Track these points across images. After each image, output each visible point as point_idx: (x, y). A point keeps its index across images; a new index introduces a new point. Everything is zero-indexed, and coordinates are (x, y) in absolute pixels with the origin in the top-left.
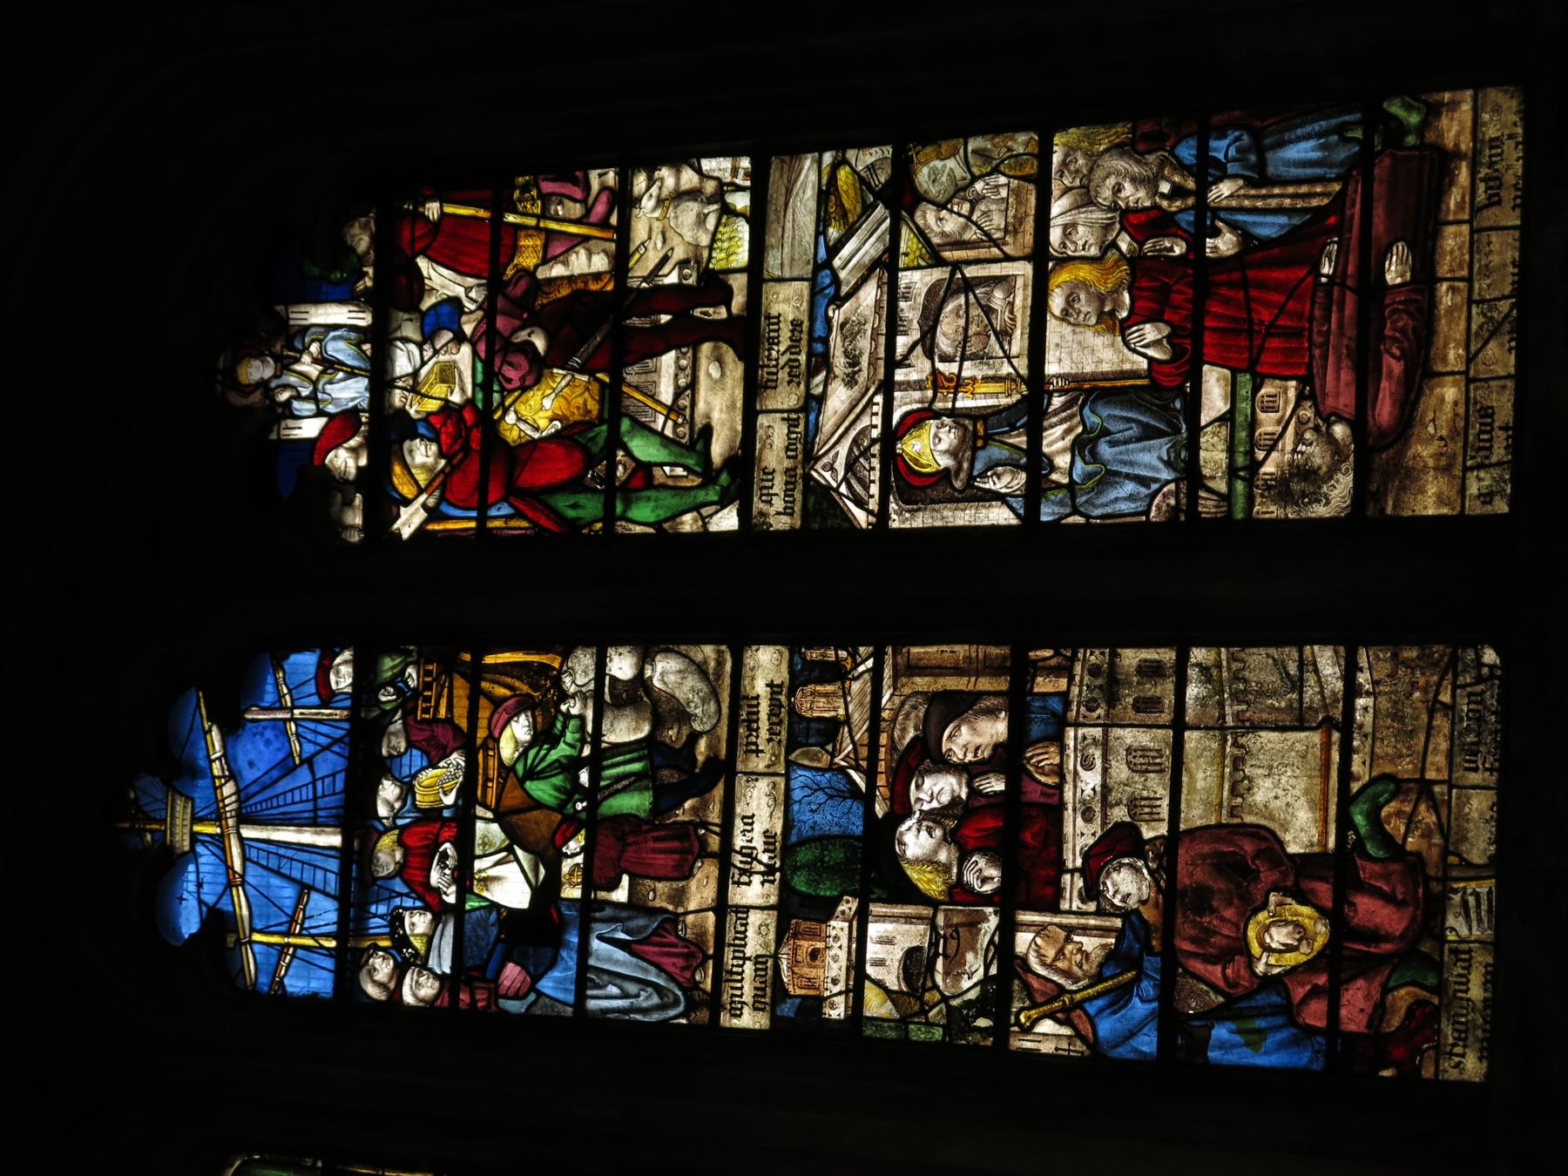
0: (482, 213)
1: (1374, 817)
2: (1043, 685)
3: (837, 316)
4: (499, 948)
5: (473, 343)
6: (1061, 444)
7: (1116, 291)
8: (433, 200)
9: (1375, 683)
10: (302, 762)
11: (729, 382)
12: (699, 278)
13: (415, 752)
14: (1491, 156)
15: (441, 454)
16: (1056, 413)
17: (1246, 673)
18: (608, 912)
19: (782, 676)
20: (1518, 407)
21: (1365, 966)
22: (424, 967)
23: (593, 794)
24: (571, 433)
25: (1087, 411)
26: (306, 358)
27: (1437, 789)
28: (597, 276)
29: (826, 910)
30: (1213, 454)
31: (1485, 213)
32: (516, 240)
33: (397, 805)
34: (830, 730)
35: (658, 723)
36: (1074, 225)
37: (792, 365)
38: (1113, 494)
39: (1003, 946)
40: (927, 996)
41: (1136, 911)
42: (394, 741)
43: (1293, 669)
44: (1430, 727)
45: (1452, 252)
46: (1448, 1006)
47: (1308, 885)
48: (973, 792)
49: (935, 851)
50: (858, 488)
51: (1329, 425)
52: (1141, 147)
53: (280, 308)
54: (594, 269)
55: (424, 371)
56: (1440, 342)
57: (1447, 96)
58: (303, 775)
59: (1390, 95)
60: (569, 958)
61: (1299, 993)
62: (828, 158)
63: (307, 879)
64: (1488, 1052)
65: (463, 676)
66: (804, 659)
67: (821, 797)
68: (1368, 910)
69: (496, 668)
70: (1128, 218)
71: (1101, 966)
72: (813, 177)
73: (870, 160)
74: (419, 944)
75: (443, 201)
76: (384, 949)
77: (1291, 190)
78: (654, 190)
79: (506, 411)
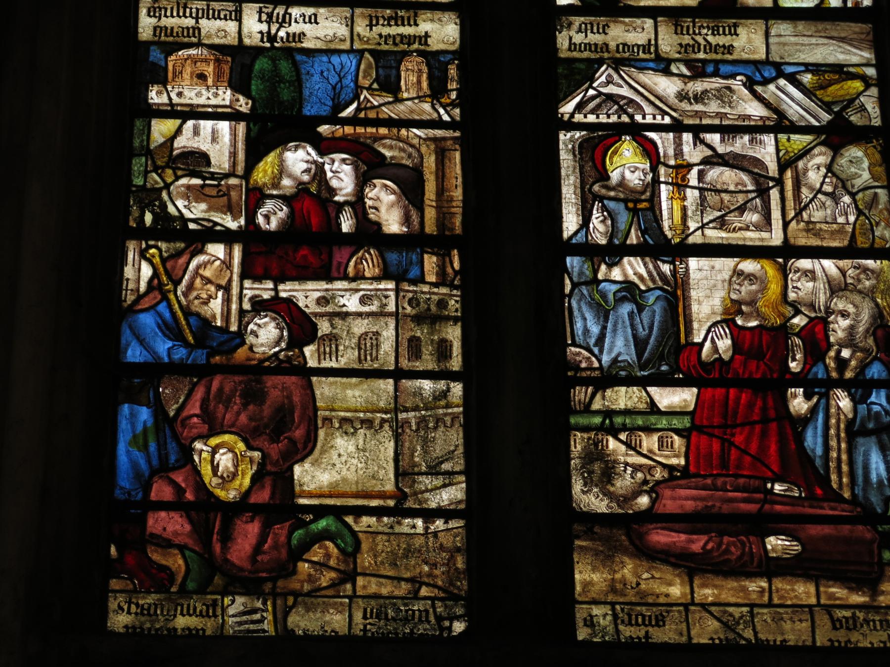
2: (430, 262)
3: (737, 84)
6: (630, 272)
7: (759, 315)
9: (435, 534)
14: (874, 621)
16: (657, 268)
17: (442, 429)
19: (435, 45)
20: (665, 647)
21: (202, 532)
25: (658, 293)
27: (349, 586)
29: (239, 85)
36: (814, 279)
37: (696, 47)
38: (589, 316)
40: (169, 172)
41: (243, 343)
43: (446, 466)
44: (400, 579)
45: (793, 590)
46: (169, 600)
47: (268, 482)
48: (340, 206)
49: (290, 176)
50: (592, 105)
51: (648, 493)
52: (880, 333)
56: (718, 581)
61: (179, 478)
62: (871, 72)
66: (448, 63)
67: (334, 80)
71: (198, 315)
72: (855, 60)
73: (869, 107)
77: (844, 457)
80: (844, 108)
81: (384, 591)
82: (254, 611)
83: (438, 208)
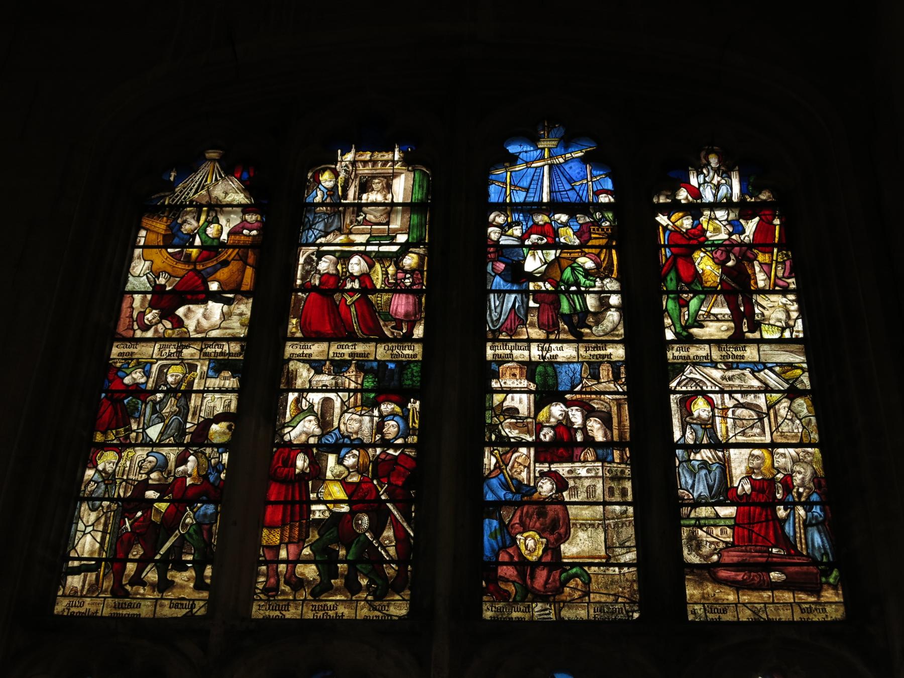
0: (777, 240)
2: (616, 454)
3: (747, 372)
7: (762, 473)
8: (781, 221)
9: (624, 574)
10: (573, 186)
11: (720, 333)
12: (757, 321)
13: (578, 227)
15: (687, 230)
16: (716, 454)
17: (625, 527)
18: (525, 300)
19: (614, 359)
21: (522, 574)
22: (502, 234)
23: (567, 292)
24: (698, 277)
25: (717, 465)
26: (719, 179)
27: (587, 598)
28: (756, 283)
29: (531, 378)
30: (704, 512)
31: (798, 607)
32: (768, 253)
33: (559, 221)
34: (596, 377)
35: (594, 314)
36: (785, 457)
37: (728, 356)
38: (687, 476)
39: (521, 443)
40: (502, 417)
41: (537, 491)
42: (582, 219)
44: (609, 594)
45: (783, 596)
46: (509, 605)
47: (550, 552)
48: (576, 430)
49: (554, 417)
50: (684, 383)
51: (717, 554)
52: (815, 480)
53: (737, 168)
54: (758, 282)
55: (717, 222)
56: (750, 593)
57: (840, 592)
58: (568, 187)
60: (508, 287)
61: (511, 551)
62: (805, 366)
63: (531, 190)
64: (493, 620)
65: (607, 243)
66: (621, 366)
67: (571, 375)
69: (611, 254)
70: (789, 477)
71: (516, 479)
72: (797, 360)
74: (510, 232)
75: (780, 225)
77: (803, 536)
78: (789, 302)
81: (603, 600)
83: (619, 430)
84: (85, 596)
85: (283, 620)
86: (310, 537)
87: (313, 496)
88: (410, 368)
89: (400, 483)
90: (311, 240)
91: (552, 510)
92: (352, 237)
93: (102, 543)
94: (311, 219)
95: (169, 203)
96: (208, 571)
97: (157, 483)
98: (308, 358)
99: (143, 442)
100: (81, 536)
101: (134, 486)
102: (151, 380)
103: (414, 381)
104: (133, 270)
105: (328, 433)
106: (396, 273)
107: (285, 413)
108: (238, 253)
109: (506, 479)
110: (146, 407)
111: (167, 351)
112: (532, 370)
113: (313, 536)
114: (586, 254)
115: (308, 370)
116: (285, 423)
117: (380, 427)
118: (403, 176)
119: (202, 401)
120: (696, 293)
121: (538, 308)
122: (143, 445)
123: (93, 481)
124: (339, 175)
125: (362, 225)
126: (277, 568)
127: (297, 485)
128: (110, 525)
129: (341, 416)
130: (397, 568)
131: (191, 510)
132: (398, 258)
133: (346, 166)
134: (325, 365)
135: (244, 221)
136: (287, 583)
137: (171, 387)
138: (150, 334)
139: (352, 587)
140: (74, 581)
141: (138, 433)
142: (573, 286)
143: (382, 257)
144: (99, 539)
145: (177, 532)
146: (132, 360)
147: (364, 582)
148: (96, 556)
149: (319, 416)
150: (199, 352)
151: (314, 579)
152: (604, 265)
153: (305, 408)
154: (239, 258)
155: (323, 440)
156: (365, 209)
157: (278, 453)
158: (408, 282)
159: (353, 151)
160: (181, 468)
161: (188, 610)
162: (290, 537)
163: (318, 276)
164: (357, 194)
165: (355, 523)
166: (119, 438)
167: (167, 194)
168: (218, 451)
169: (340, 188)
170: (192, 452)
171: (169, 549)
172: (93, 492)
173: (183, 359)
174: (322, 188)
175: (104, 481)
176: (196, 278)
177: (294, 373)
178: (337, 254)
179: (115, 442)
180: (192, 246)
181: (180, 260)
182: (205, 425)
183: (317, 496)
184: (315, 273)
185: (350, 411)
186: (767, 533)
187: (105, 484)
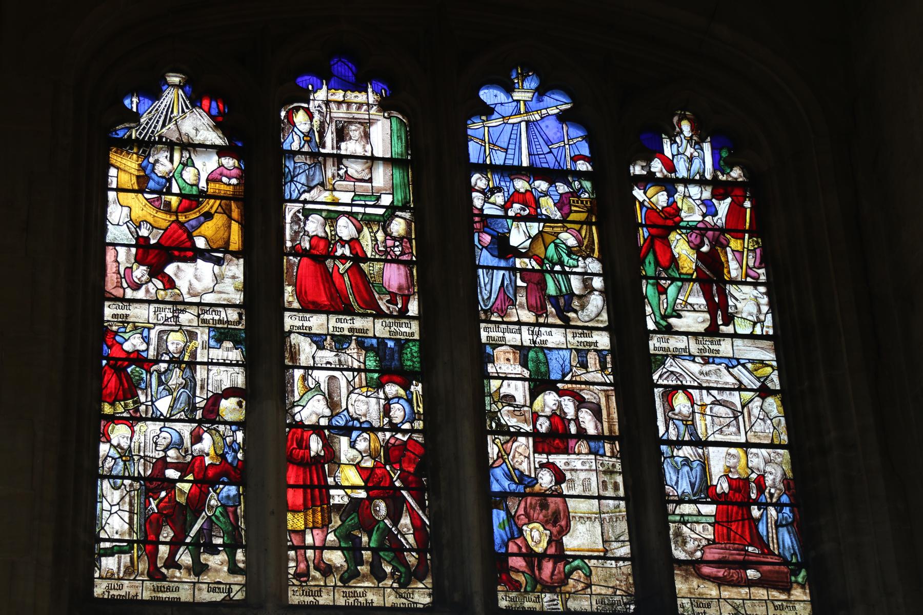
0: (748, 225)
1: (577, 568)
2: (607, 446)
3: (722, 367)
4: (496, 233)
5: (702, 221)
6: (686, 453)
7: (738, 473)
8: (752, 204)
9: (620, 568)
10: (550, 149)
11: (697, 325)
12: (731, 313)
13: (558, 198)
15: (663, 208)
16: (696, 451)
17: (618, 522)
18: (513, 278)
19: (600, 347)
21: (530, 565)
22: (485, 202)
23: (552, 272)
24: (674, 261)
25: (698, 462)
26: (692, 150)
27: (589, 590)
28: (729, 272)
29: (524, 364)
30: (687, 509)
32: (739, 239)
33: (539, 189)
34: (584, 365)
35: (580, 297)
36: (758, 457)
37: (704, 350)
38: (672, 472)
39: (519, 433)
40: (500, 404)
41: (537, 483)
42: (562, 188)
43: (622, 538)
44: (608, 587)
46: (521, 595)
47: (553, 544)
48: (569, 421)
49: (548, 407)
50: (665, 376)
51: (700, 550)
52: (785, 482)
53: (709, 139)
54: (731, 271)
55: (691, 200)
56: (730, 589)
57: (808, 591)
58: (546, 150)
59: (807, 571)
60: (494, 262)
61: (519, 542)
62: (774, 364)
63: (510, 151)
64: (508, 610)
65: (587, 217)
66: (606, 355)
67: (561, 362)
68: (548, 566)
69: (591, 230)
70: (761, 478)
71: (518, 469)
72: (768, 358)
73: (775, 380)
74: (492, 200)
75: (751, 208)
76: (488, 185)
77: (775, 536)
78: (760, 295)
79: (680, 235)
80: (766, 380)
81: (603, 592)
82: (554, 600)
83: (608, 422)
84: (122, 579)
85: (317, 607)
86: (333, 523)
87: (330, 480)
88: (409, 347)
89: (411, 470)
90: (295, 195)
91: (553, 502)
92: (336, 194)
93: (131, 524)
94: (292, 170)
95: (136, 137)
96: (240, 555)
97: (176, 461)
98: (308, 331)
99: (154, 416)
100: (108, 516)
101: (153, 464)
102: (151, 348)
103: (414, 362)
104: (110, 216)
105: (337, 414)
106: (385, 241)
107: (293, 391)
108: (220, 205)
109: (509, 469)
110: (151, 377)
111: (163, 314)
112: (524, 355)
113: (336, 522)
114: (568, 229)
115: (310, 345)
116: (294, 402)
117: (387, 411)
118: (379, 123)
119: (208, 374)
120: (673, 280)
121: (526, 287)
122: (154, 419)
123: (110, 457)
124: (313, 117)
125: (344, 180)
126: (305, 553)
127: (314, 468)
128: (136, 505)
129: (348, 397)
130: (417, 556)
131: (215, 491)
132: (385, 222)
133: (319, 106)
134: (326, 340)
135: (221, 166)
136: (316, 568)
137: (174, 357)
138: (141, 294)
139: (378, 574)
140: (109, 563)
141: (147, 406)
142: (557, 264)
143: (369, 220)
144: (127, 521)
145: (204, 513)
146: (128, 323)
147: (388, 569)
148: (127, 537)
149: (327, 396)
150: (196, 318)
151: (342, 566)
152: (585, 243)
153: (312, 386)
154: (222, 211)
155: (334, 422)
156: (345, 161)
157: (291, 433)
158: (398, 251)
159: (325, 87)
160: (197, 447)
161: (226, 594)
162: (314, 522)
163: (307, 238)
164: (335, 142)
165: (374, 510)
166: (129, 410)
167: (132, 125)
168: (231, 429)
169: (316, 134)
170: (205, 429)
171: (199, 531)
172: (111, 469)
173: (181, 325)
174: (299, 133)
175: (121, 457)
176: (180, 231)
177: (297, 347)
178: (324, 214)
179: (125, 415)
180: (169, 192)
181: (160, 209)
182: (214, 401)
183: (335, 480)
184: (304, 235)
185: (356, 391)
186: (743, 532)
187: (122, 460)
